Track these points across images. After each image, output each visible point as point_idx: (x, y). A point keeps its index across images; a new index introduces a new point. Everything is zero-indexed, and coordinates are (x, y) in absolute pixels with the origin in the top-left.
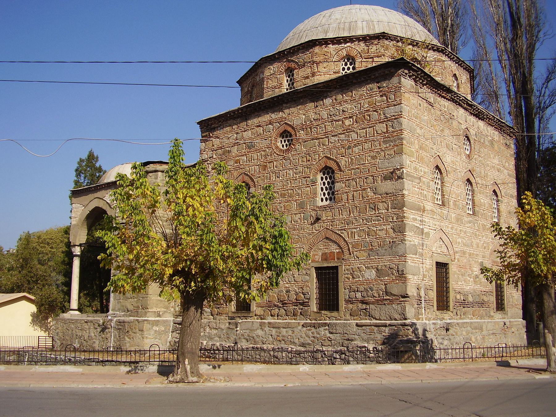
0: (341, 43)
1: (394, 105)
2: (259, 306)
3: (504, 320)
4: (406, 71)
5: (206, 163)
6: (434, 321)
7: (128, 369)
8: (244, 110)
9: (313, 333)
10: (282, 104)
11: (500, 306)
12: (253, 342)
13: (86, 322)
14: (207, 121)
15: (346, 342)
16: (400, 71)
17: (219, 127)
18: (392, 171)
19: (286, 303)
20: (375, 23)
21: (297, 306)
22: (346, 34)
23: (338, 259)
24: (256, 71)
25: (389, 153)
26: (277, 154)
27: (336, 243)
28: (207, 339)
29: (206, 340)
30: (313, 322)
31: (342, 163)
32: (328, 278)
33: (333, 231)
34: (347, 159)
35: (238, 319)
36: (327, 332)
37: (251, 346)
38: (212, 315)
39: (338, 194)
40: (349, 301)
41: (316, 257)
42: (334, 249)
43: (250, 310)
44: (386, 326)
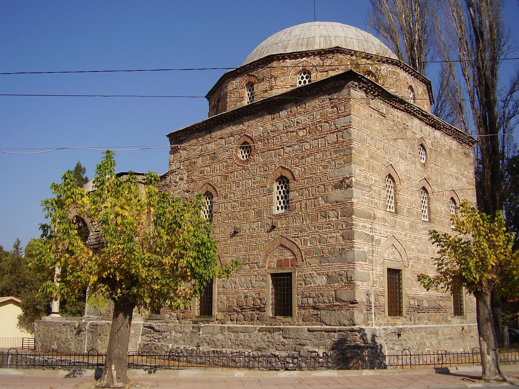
0: (297, 58)
1: (344, 116)
2: (220, 311)
3: (462, 325)
4: (356, 83)
5: (174, 174)
6: (385, 327)
7: (67, 373)
8: (209, 123)
9: (268, 338)
10: (242, 117)
11: (458, 311)
12: (214, 346)
13: (64, 325)
14: (175, 134)
15: (298, 347)
16: (349, 83)
17: (187, 139)
18: (341, 179)
19: (244, 308)
20: (332, 38)
21: (254, 311)
22: (304, 49)
23: (292, 265)
24: (221, 86)
25: (339, 162)
26: (238, 165)
27: (290, 250)
28: (173, 342)
29: (171, 343)
30: (269, 327)
31: (296, 173)
32: (283, 283)
33: (287, 239)
34: (300, 169)
35: (201, 323)
36: (281, 336)
37: (212, 349)
38: (178, 319)
39: (292, 203)
40: (302, 307)
41: (272, 263)
42: (288, 256)
43: (211, 315)
44: (335, 332)
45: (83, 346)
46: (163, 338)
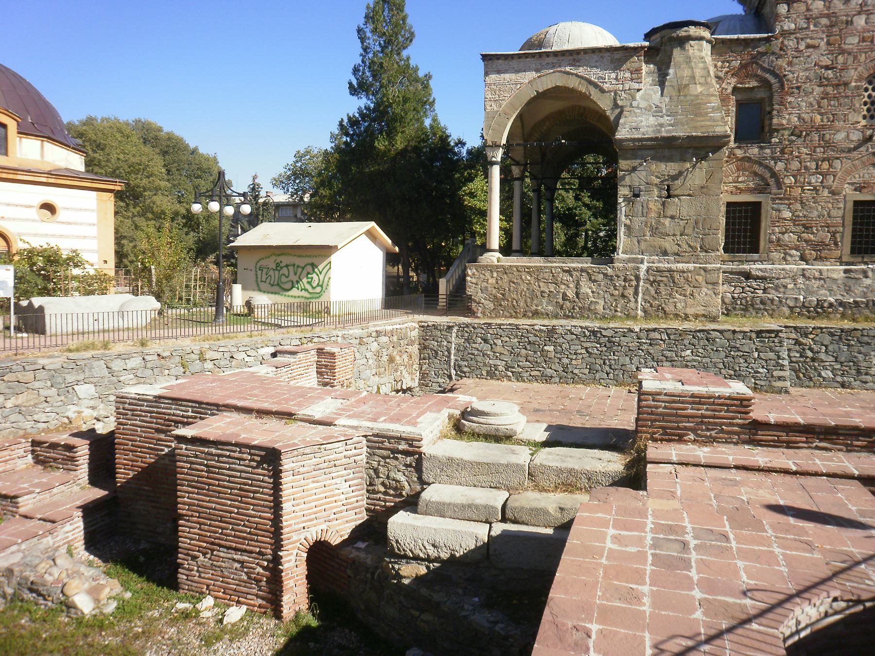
5: (792, 37)
28: (803, 293)
29: (800, 294)
45: (632, 305)
46: (776, 288)
